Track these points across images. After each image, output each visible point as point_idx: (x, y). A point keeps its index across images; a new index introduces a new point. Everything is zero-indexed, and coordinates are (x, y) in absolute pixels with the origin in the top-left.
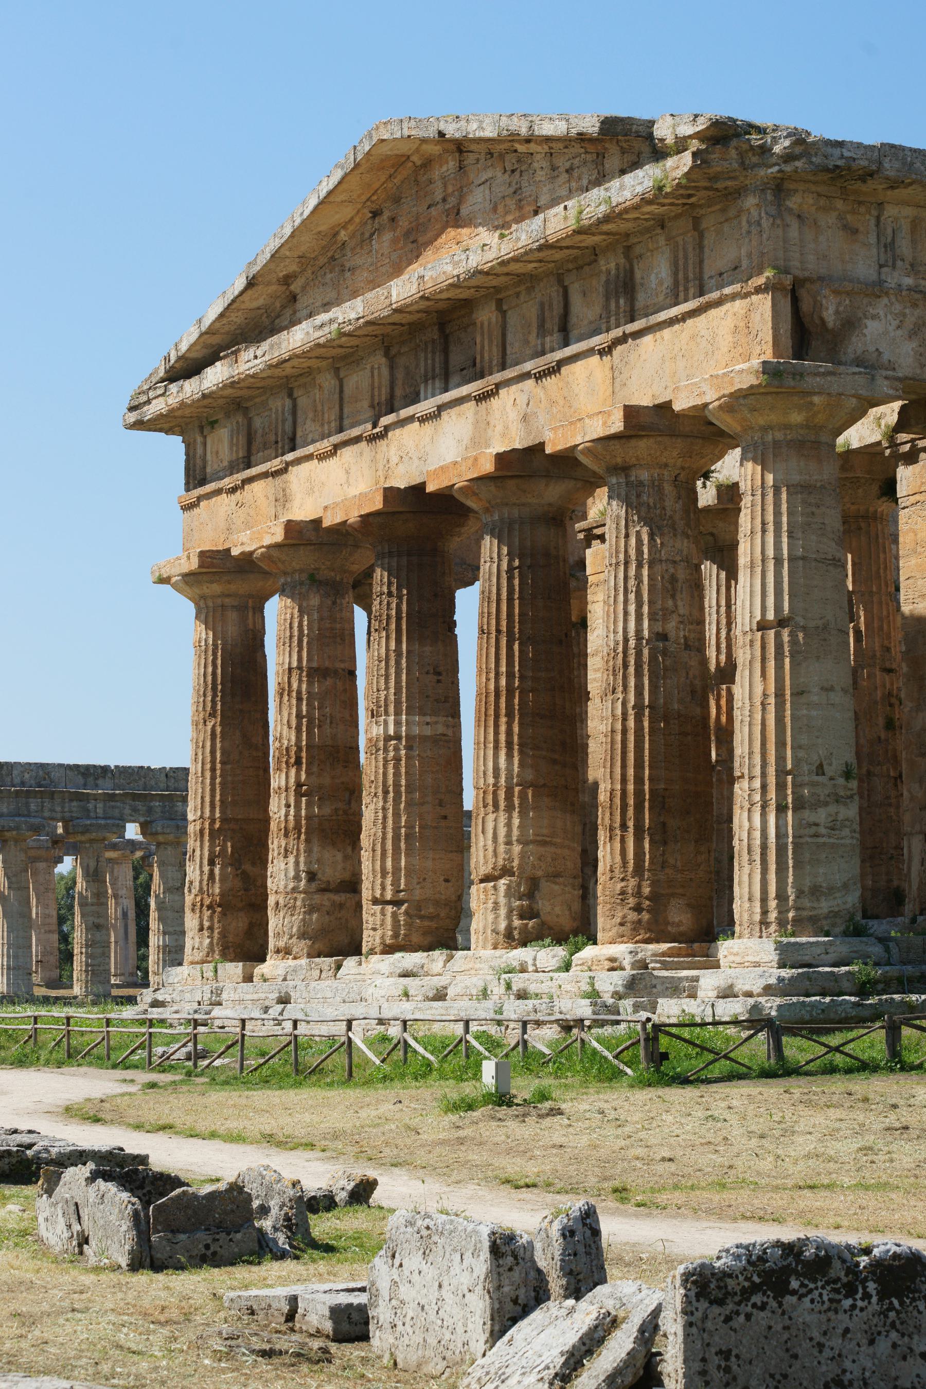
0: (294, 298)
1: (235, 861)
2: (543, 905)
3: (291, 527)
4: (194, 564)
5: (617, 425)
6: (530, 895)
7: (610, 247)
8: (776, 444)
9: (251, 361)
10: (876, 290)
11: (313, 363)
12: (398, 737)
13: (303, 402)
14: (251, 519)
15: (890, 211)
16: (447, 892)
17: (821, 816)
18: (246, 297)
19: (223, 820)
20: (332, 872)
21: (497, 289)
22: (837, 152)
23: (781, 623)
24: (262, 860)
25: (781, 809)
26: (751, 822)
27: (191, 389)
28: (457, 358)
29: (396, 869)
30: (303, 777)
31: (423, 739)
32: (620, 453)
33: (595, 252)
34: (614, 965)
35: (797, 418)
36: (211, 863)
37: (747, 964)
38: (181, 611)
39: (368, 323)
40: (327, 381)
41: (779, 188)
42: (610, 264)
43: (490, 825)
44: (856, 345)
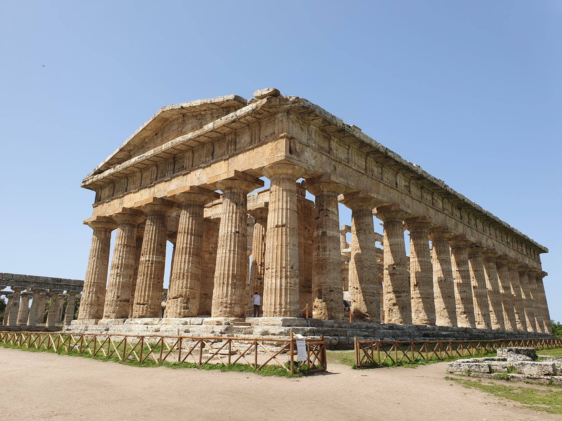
3: (124, 209)
4: (95, 218)
6: (187, 303)
7: (230, 133)
8: (283, 179)
9: (119, 167)
11: (135, 169)
12: (149, 261)
14: (113, 208)
15: (311, 126)
18: (118, 154)
19: (94, 283)
21: (193, 147)
22: (307, 103)
25: (281, 278)
27: (100, 176)
29: (145, 295)
30: (119, 271)
33: (225, 135)
34: (219, 323)
35: (290, 172)
36: (89, 293)
38: (90, 231)
39: (154, 156)
40: (138, 175)
41: (288, 112)
43: (177, 283)
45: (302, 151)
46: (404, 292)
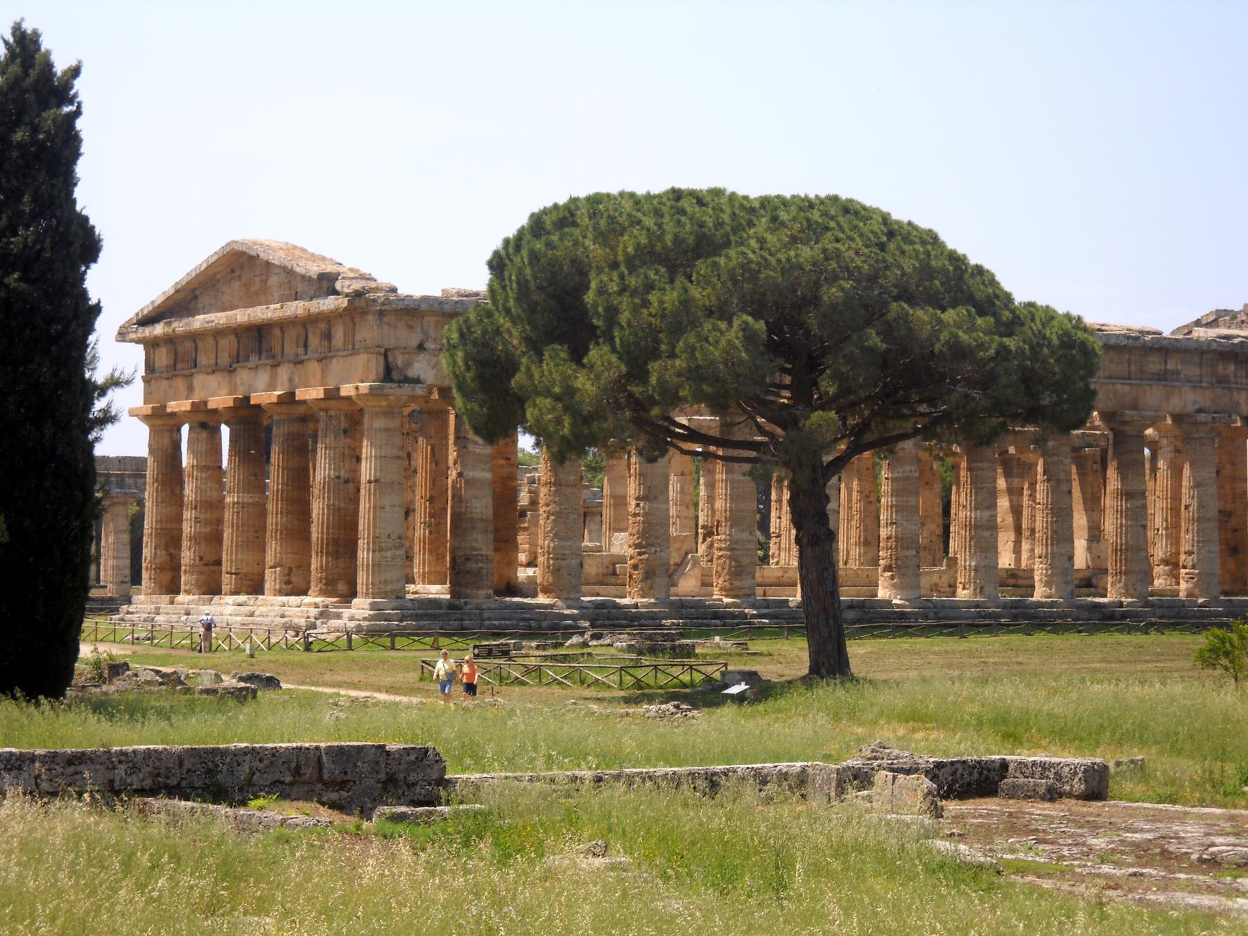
0: (196, 297)
1: (167, 548)
2: (294, 579)
5: (322, 396)
6: (289, 574)
8: (377, 413)
13: (200, 345)
16: (257, 569)
17: (389, 554)
20: (210, 557)
23: (376, 481)
24: (179, 547)
26: (364, 555)
28: (265, 346)
31: (249, 504)
32: (323, 405)
34: (316, 606)
37: (361, 608)
40: (211, 341)
41: (381, 314)
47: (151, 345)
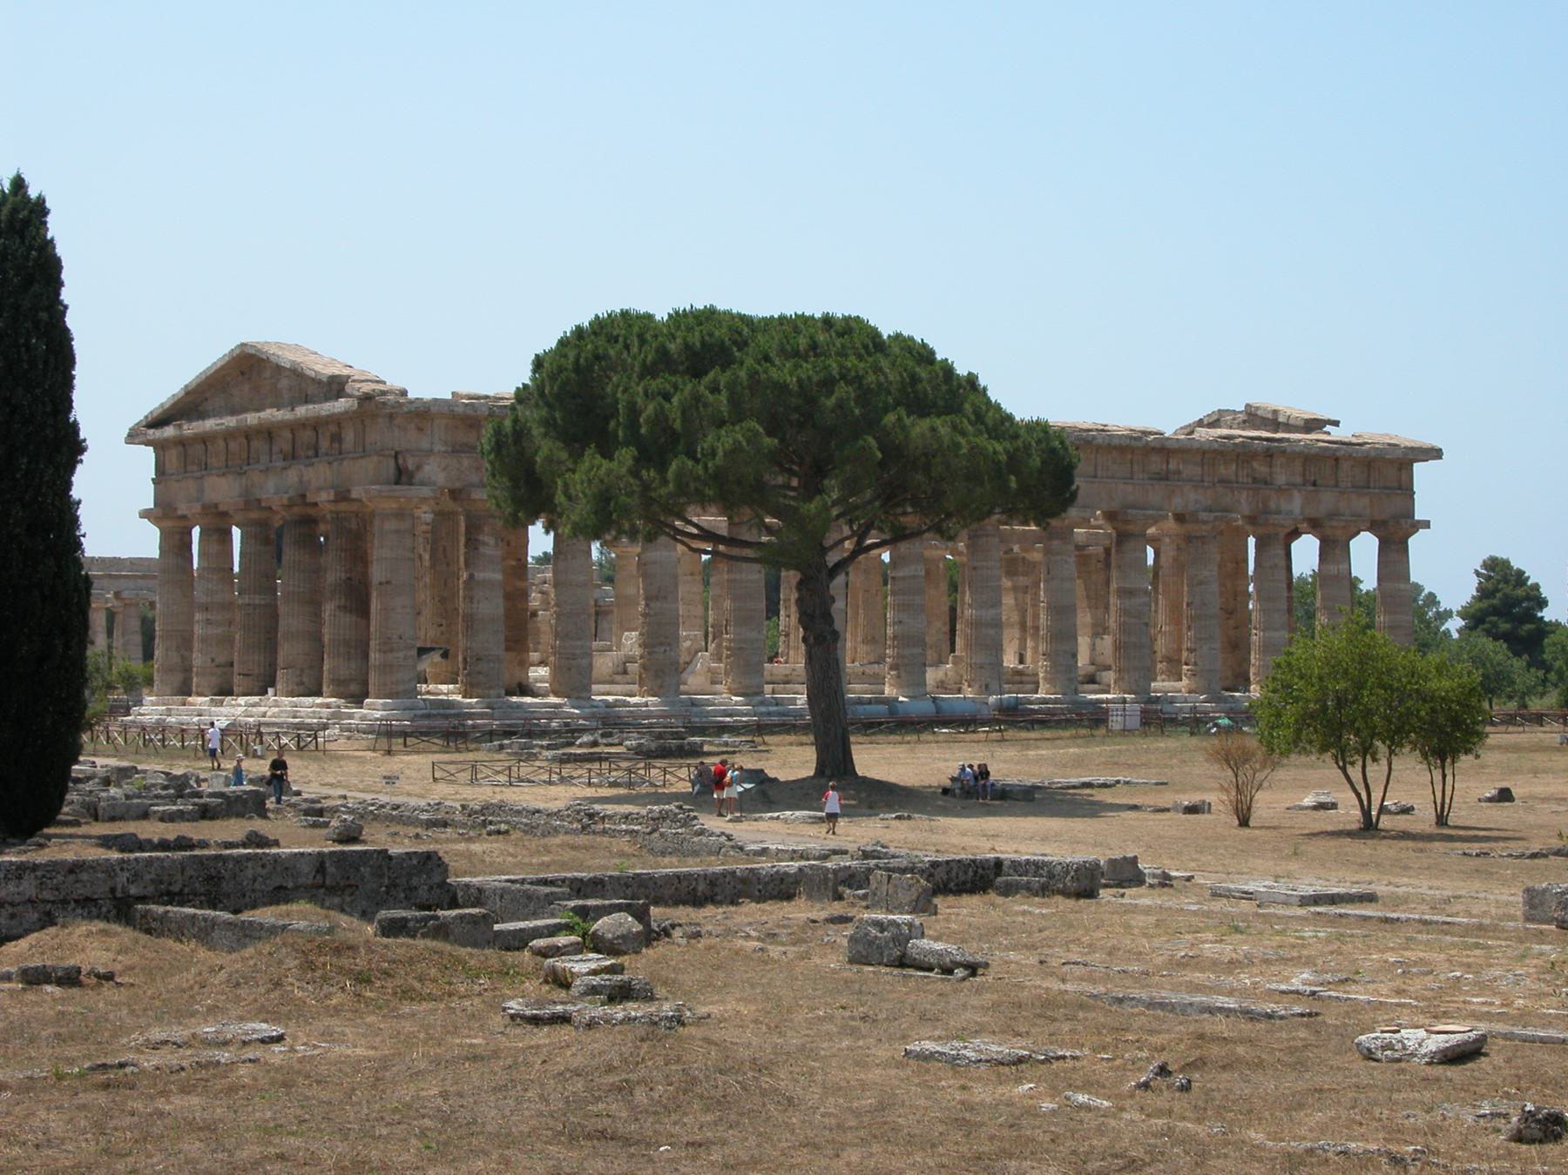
10: (430, 452)
17: (401, 655)
20: (221, 659)
24: (190, 649)
34: (328, 706)
35: (394, 506)
40: (221, 443)
42: (333, 428)
44: (419, 476)
45: (419, 467)
46: (661, 644)
47: (160, 447)
